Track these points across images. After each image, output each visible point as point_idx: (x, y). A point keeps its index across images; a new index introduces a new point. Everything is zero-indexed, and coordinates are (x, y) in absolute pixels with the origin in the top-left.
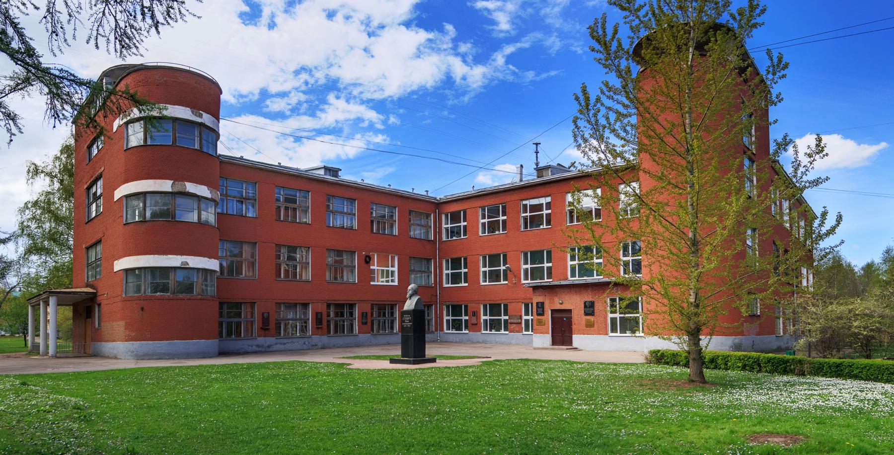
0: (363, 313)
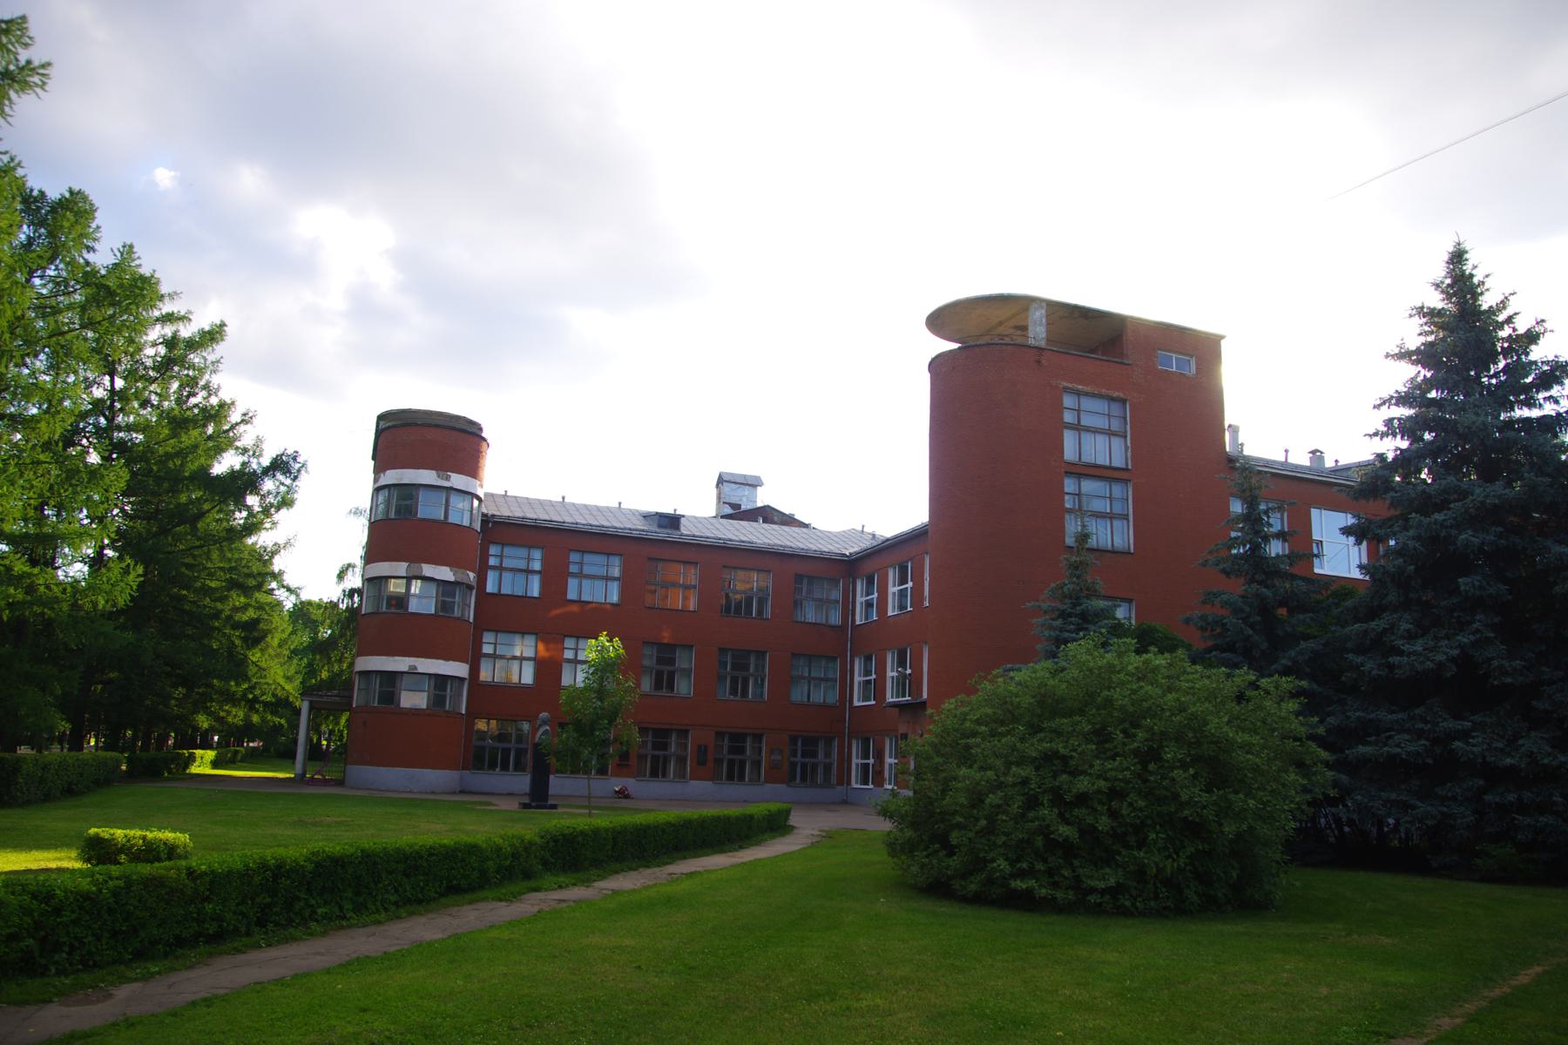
0: (700, 746)
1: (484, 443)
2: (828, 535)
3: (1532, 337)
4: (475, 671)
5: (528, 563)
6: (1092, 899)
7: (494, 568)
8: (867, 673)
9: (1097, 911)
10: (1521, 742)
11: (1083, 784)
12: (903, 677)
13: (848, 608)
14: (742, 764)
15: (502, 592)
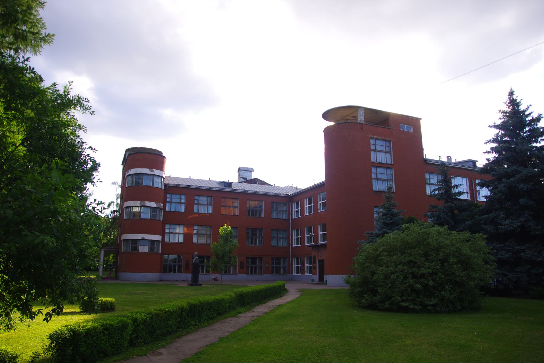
0: (241, 262)
1: (165, 159)
2: (279, 188)
3: (538, 119)
4: (163, 238)
5: (180, 200)
6: (428, 308)
7: (168, 202)
8: (298, 235)
9: (429, 312)
10: (542, 253)
11: (423, 271)
12: (311, 236)
13: (290, 213)
14: (256, 268)
15: (172, 210)
